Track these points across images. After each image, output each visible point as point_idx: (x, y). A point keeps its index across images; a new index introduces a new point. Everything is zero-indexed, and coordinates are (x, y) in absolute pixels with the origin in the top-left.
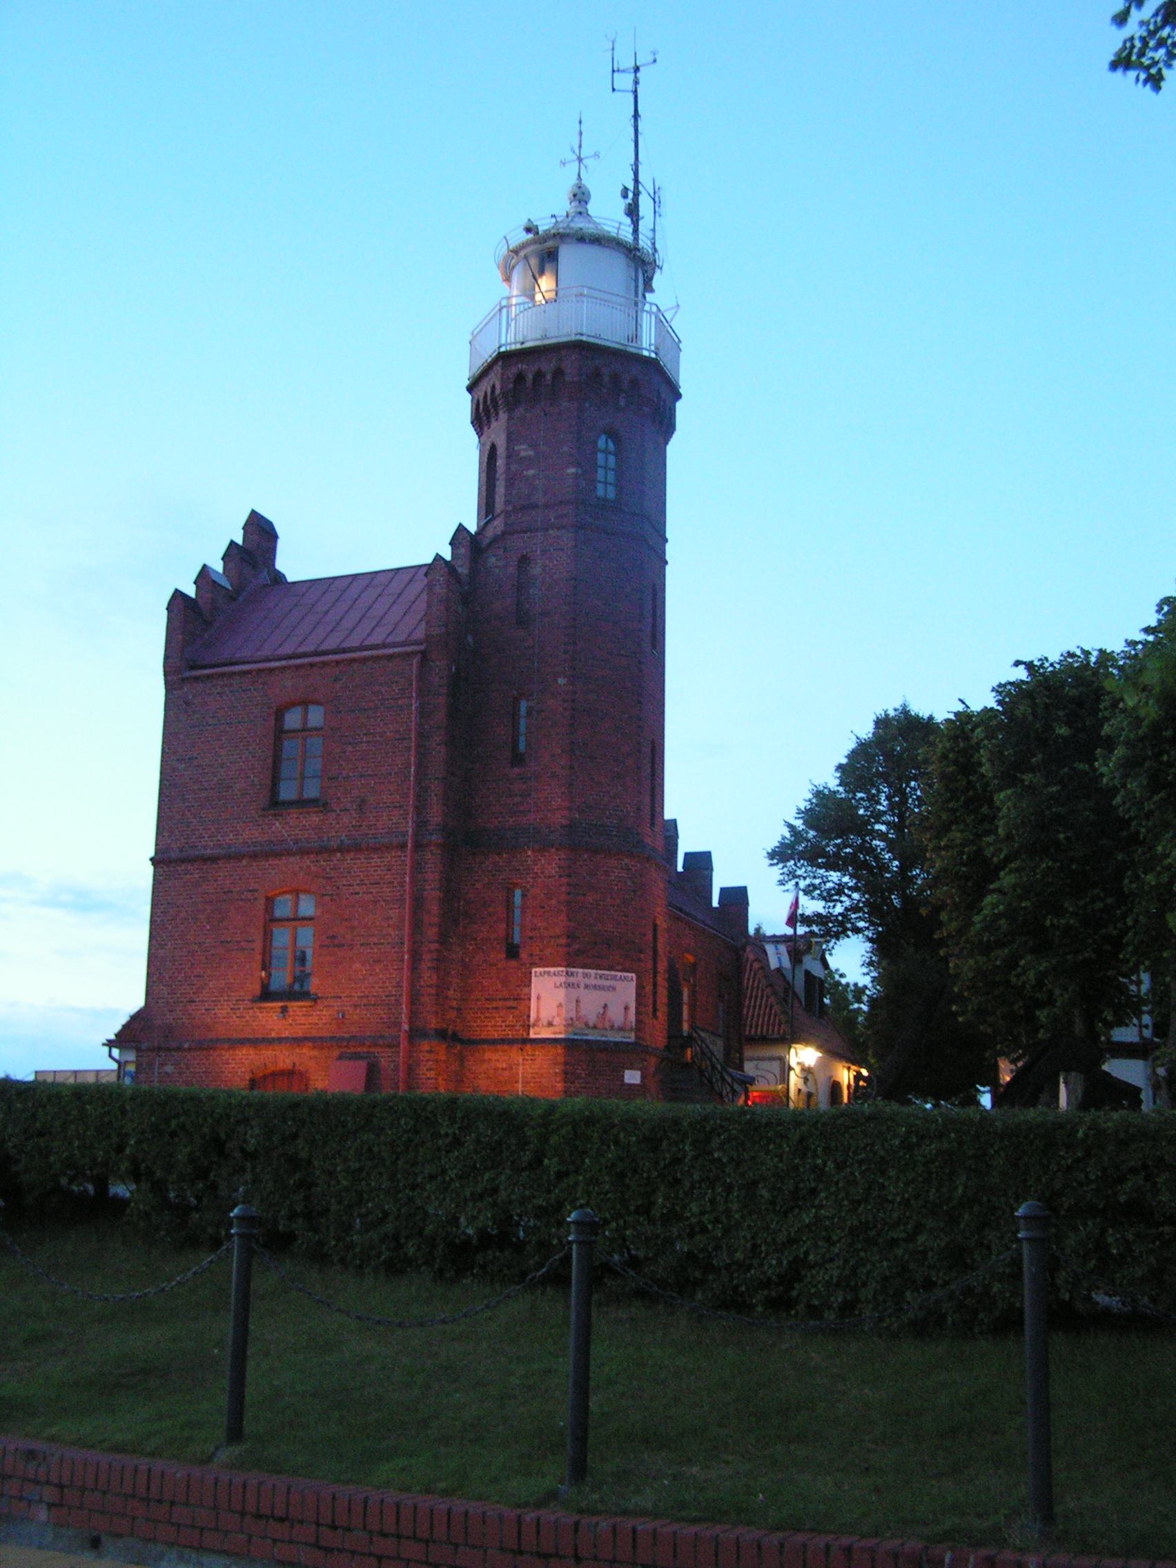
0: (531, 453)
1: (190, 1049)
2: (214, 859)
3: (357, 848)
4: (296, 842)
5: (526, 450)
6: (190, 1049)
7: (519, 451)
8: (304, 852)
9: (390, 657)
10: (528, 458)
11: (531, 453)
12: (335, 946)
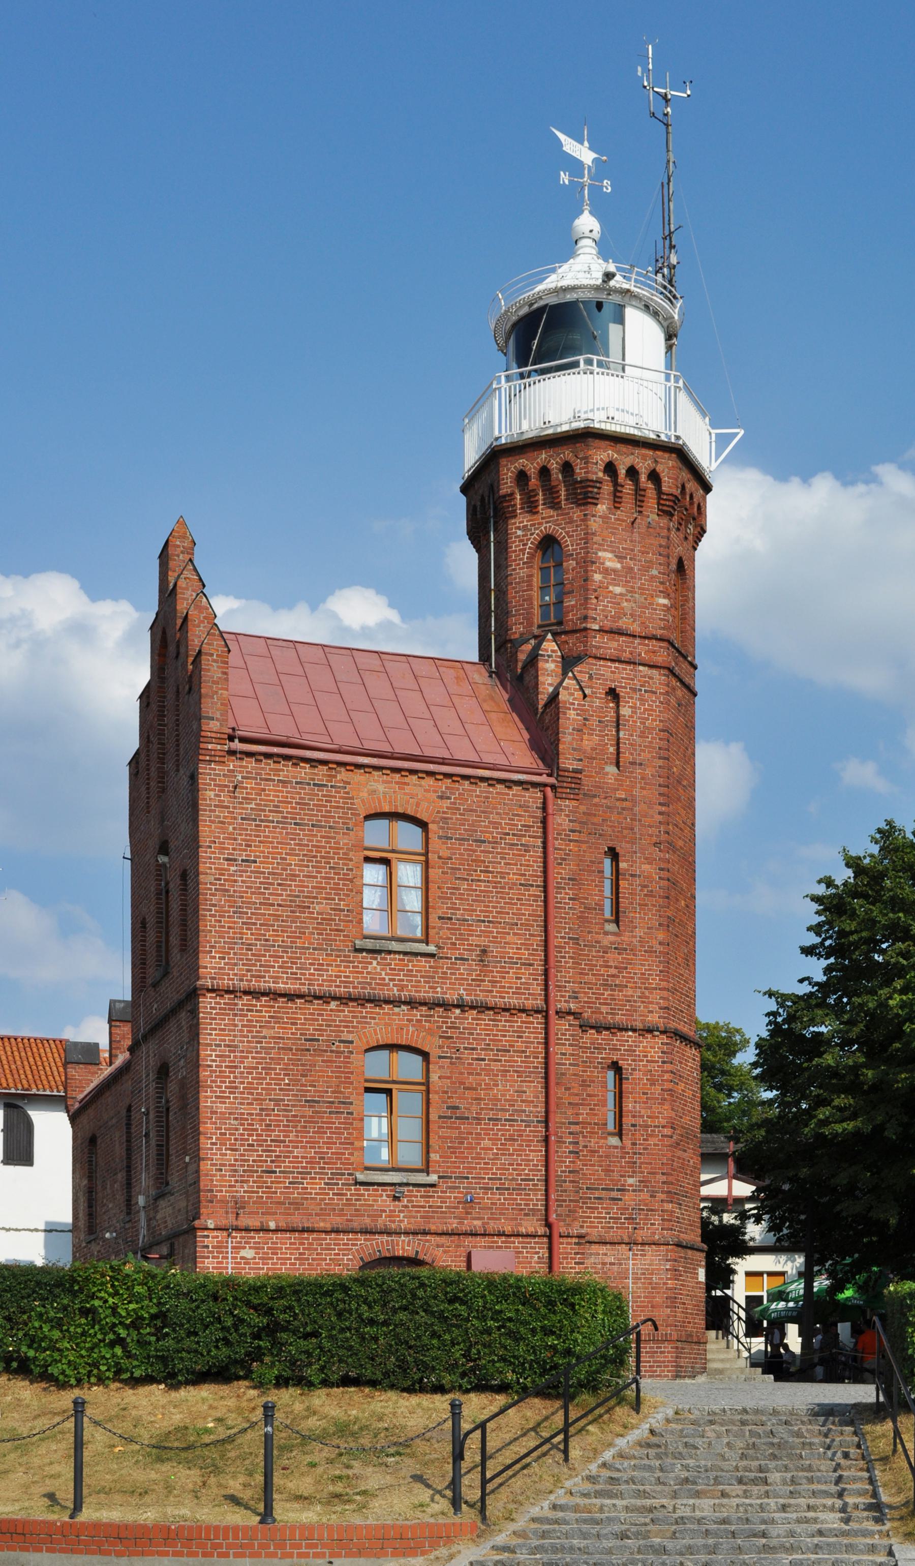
0: (619, 566)
1: (276, 1231)
2: (291, 997)
3: (482, 1008)
4: (402, 988)
5: (610, 560)
6: (276, 1231)
7: (605, 559)
8: (412, 1003)
9: (508, 783)
10: (615, 571)
11: (619, 566)
12: (457, 1118)
